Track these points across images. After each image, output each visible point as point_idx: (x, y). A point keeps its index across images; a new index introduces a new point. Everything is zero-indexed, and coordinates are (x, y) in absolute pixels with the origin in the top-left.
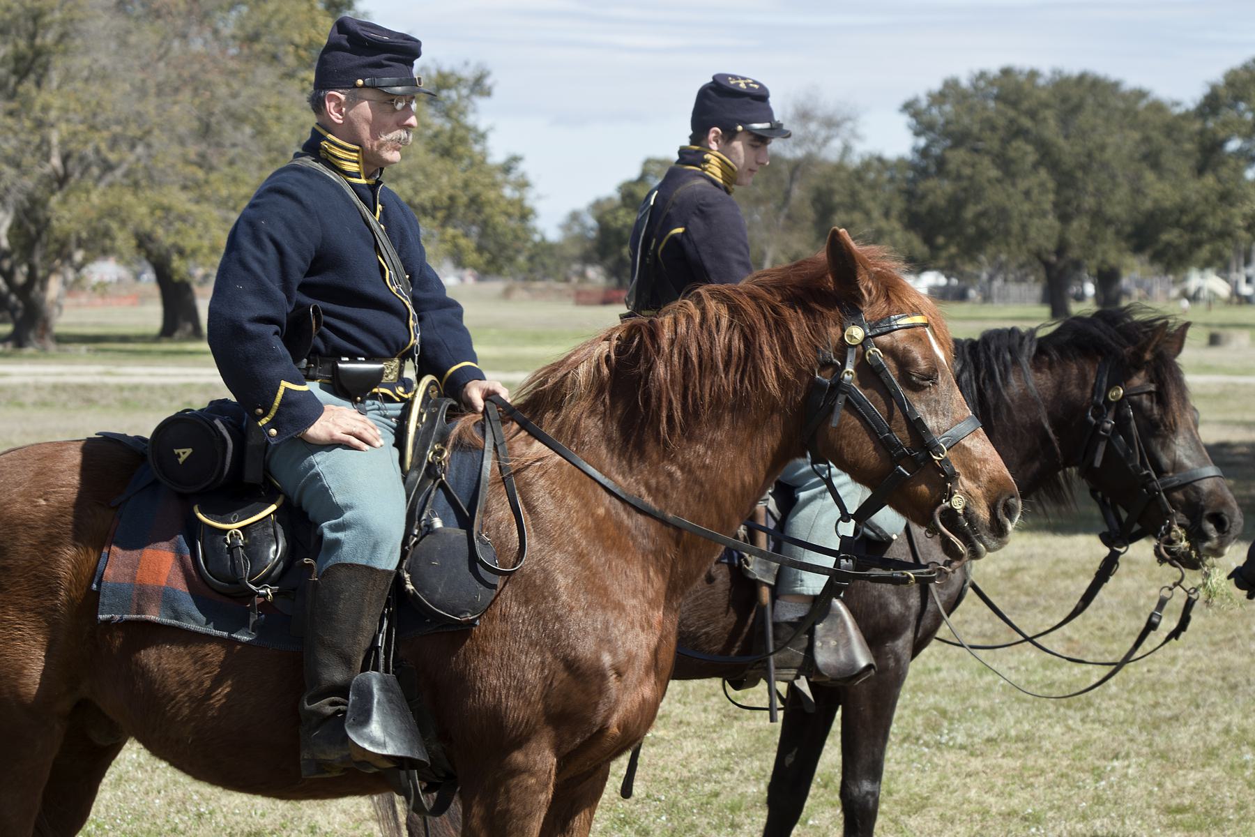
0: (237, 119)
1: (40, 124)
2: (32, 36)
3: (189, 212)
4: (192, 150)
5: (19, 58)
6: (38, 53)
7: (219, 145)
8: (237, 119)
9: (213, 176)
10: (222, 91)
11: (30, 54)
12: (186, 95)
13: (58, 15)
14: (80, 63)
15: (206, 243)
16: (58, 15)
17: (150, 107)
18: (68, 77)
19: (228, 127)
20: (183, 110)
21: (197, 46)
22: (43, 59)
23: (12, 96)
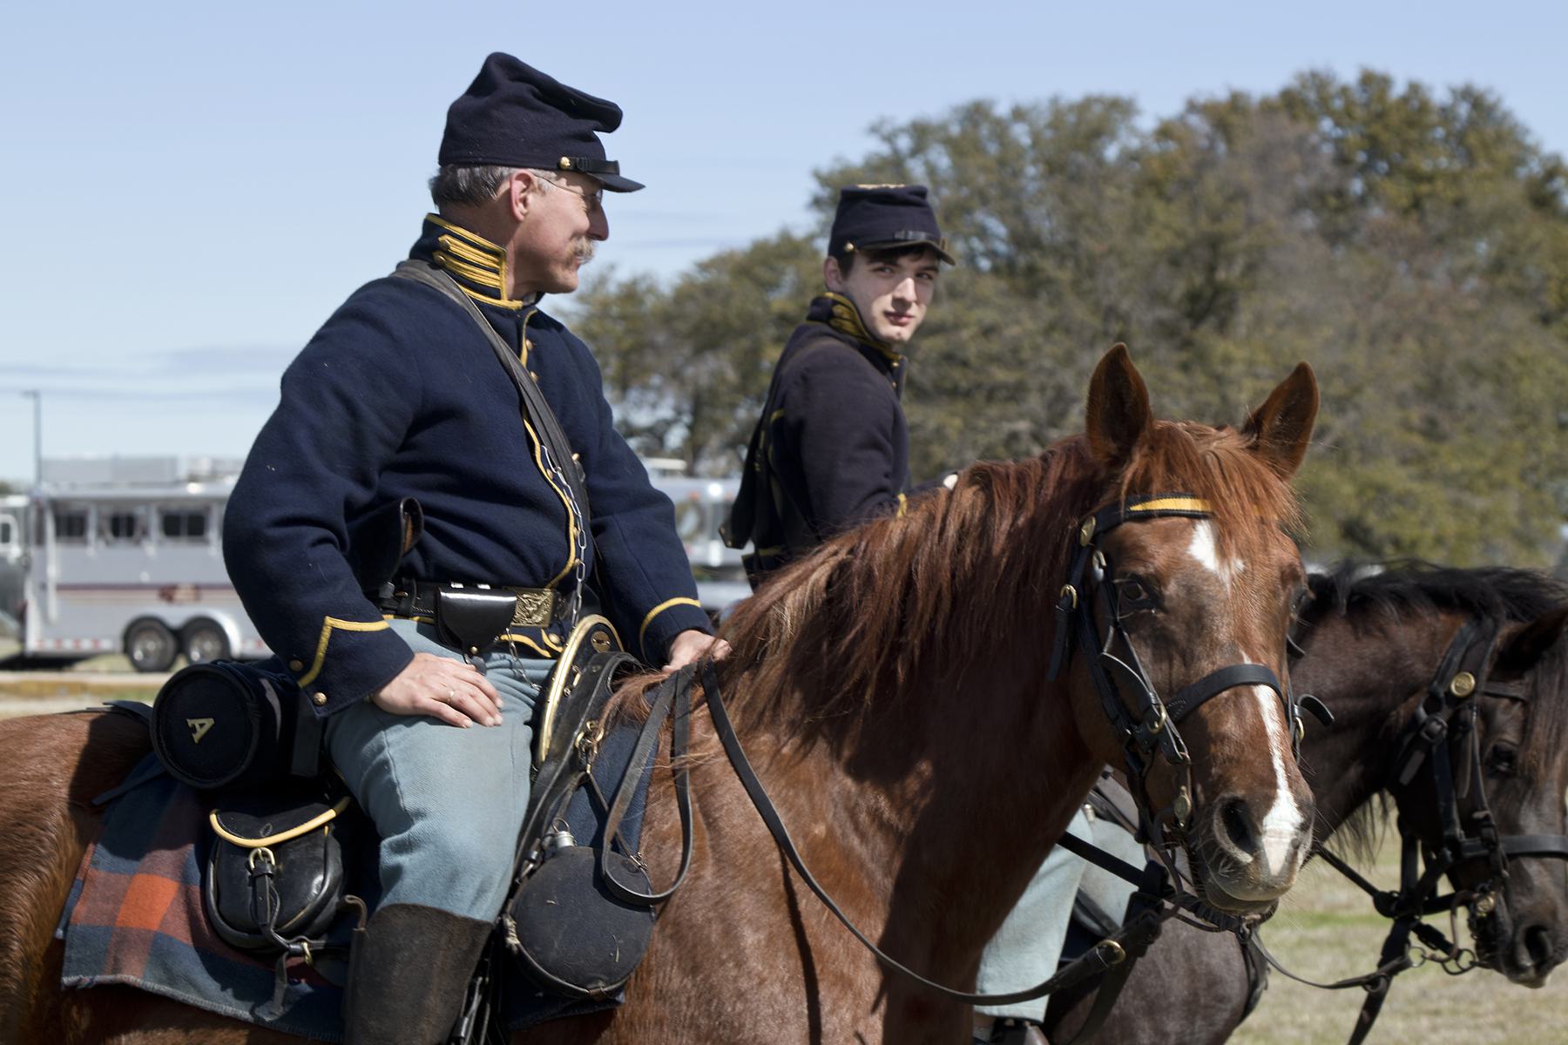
0: (1475, 373)
1: (1219, 379)
2: (1211, 269)
3: (1409, 493)
4: (1416, 415)
5: (1193, 297)
6: (1218, 290)
7: (1450, 407)
8: (1475, 373)
9: (1444, 449)
10: (1456, 337)
11: (1208, 293)
12: (1410, 344)
13: (1244, 241)
14: (1275, 303)
15: (1430, 532)
16: (1244, 241)
17: (1358, 357)
18: (1259, 320)
19: (1462, 382)
20: (1403, 365)
21: (1439, 282)
22: (1222, 300)
23: (1187, 344)
